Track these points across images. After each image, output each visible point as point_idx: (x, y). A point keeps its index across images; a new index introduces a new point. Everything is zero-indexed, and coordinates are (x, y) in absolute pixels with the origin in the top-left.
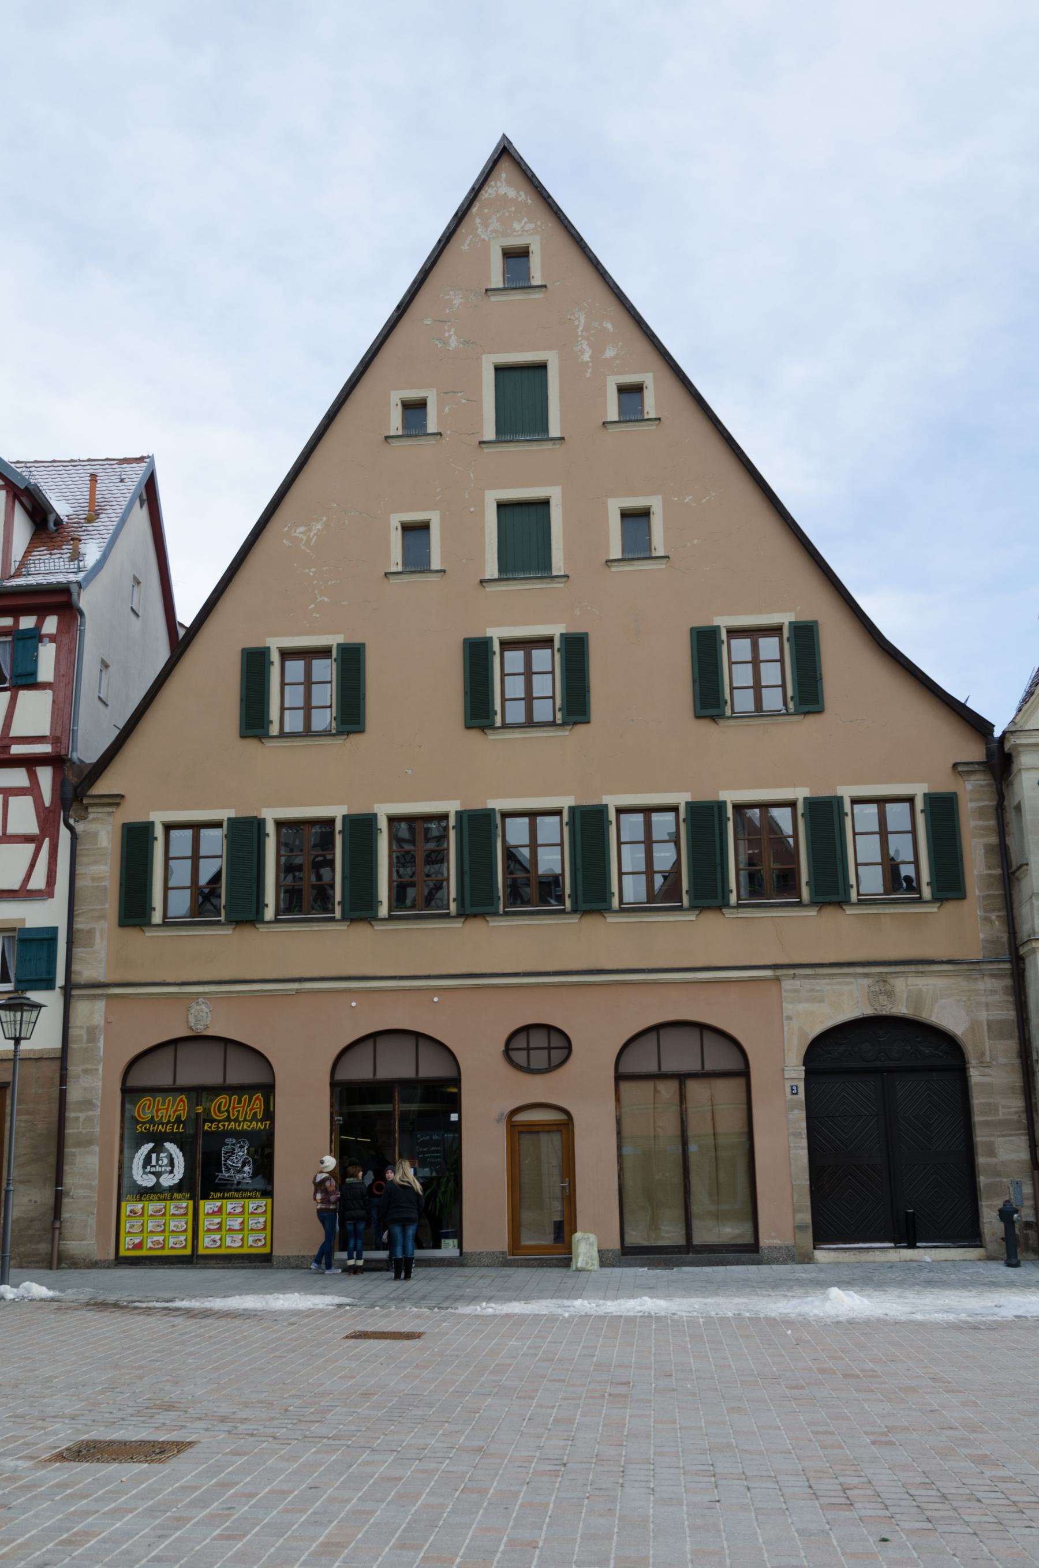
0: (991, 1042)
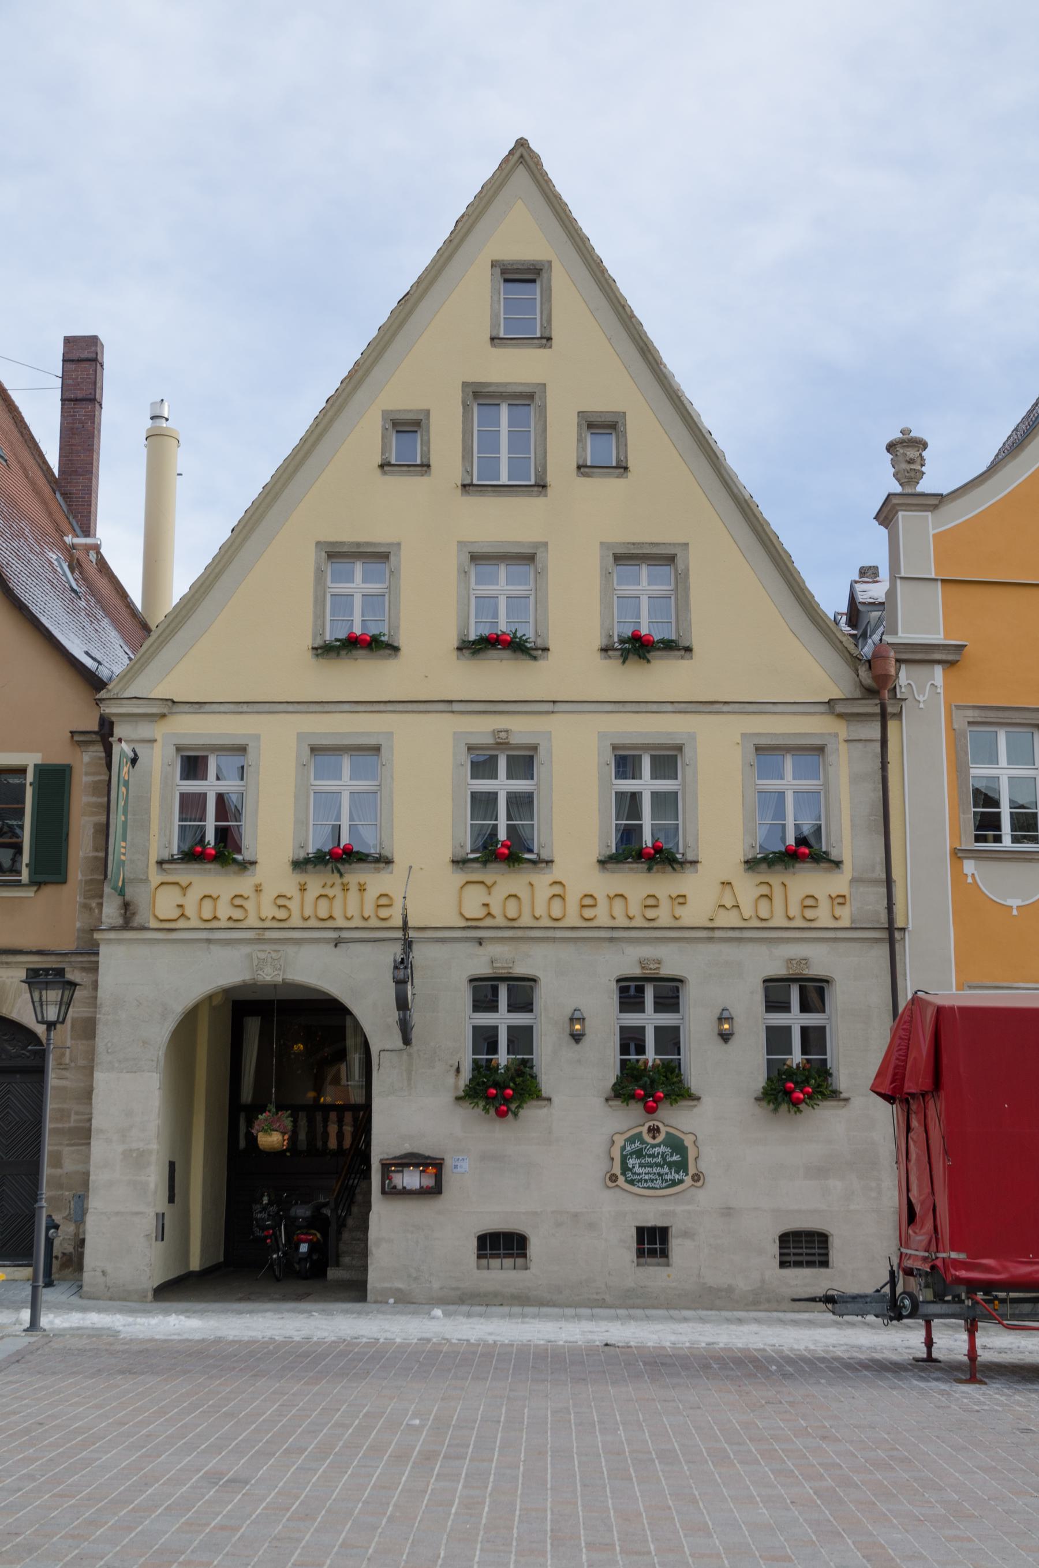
0: (73, 1042)
